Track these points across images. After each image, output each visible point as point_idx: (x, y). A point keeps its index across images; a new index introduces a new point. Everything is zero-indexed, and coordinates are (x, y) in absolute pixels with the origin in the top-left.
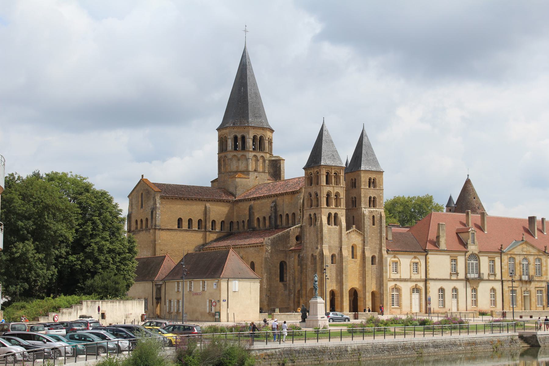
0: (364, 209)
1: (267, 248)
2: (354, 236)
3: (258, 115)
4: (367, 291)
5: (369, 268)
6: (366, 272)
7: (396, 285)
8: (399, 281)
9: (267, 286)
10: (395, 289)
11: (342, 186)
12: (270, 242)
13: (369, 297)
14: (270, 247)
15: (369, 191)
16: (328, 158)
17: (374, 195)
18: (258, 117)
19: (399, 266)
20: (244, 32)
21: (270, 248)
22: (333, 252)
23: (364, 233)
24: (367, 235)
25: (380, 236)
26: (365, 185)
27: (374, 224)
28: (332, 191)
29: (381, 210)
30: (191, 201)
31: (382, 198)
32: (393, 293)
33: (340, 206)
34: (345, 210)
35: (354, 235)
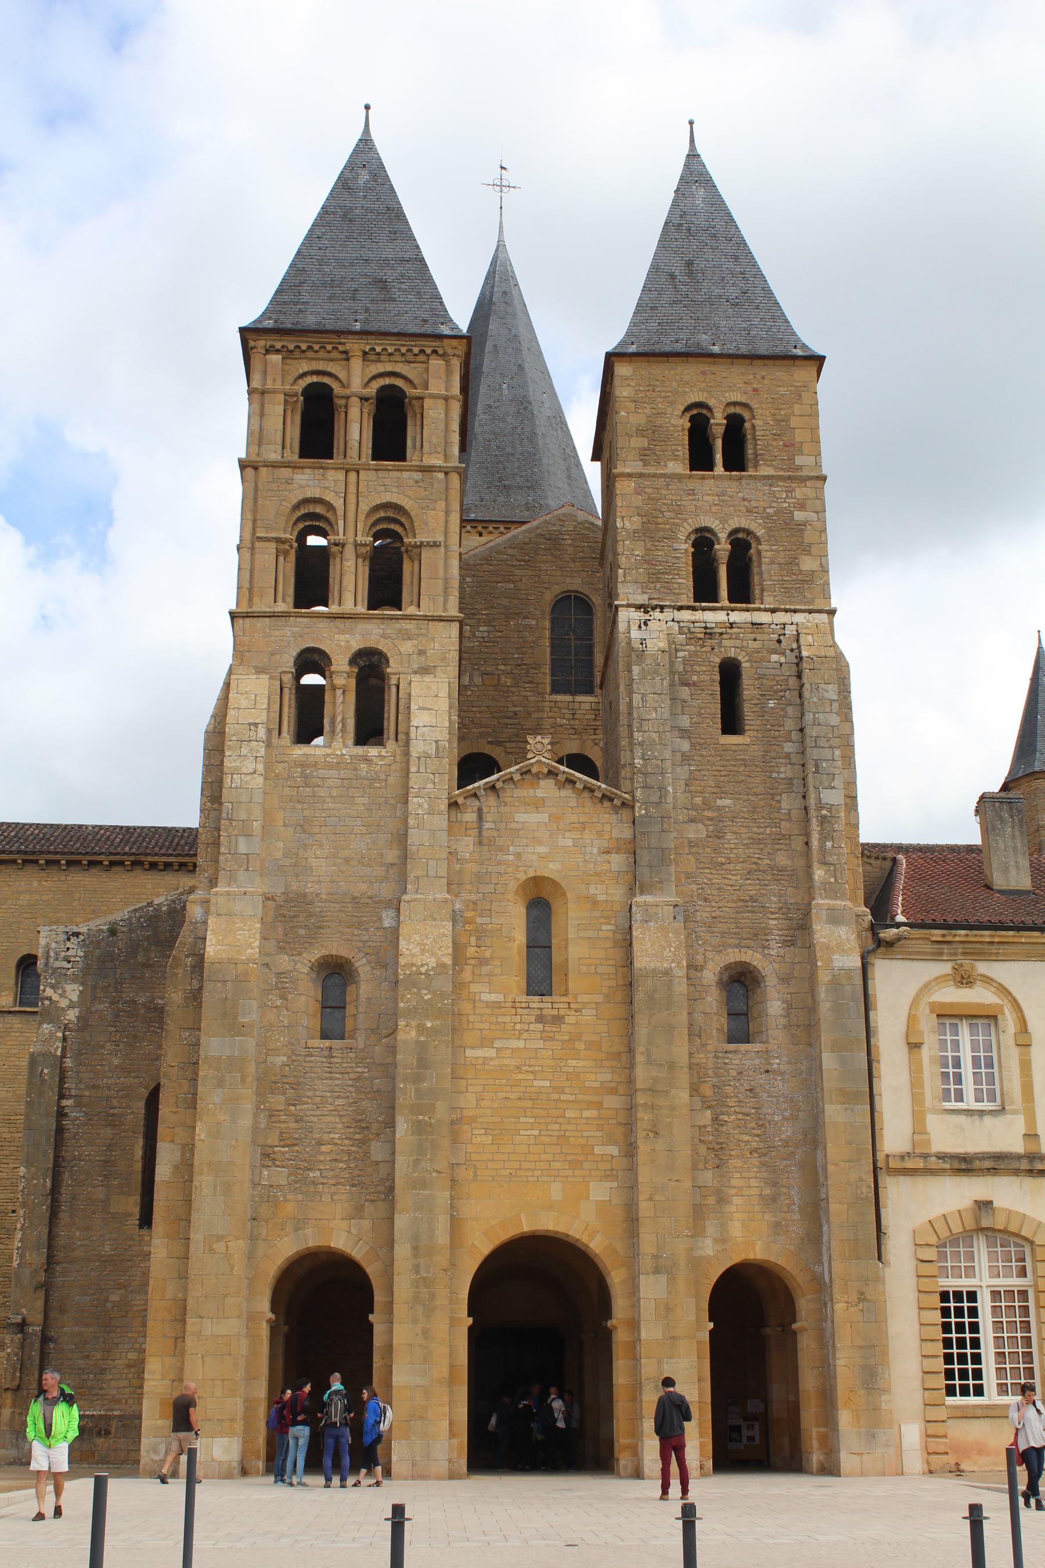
0: (637, 615)
1: (49, 992)
2: (544, 817)
3: (518, 479)
4: (646, 1263)
5: (672, 1066)
6: (641, 1099)
7: (984, 1206)
8: (1016, 1172)
9: (22, 1256)
10: (981, 1249)
11: (438, 461)
12: (76, 951)
13: (667, 1309)
14: (73, 991)
15: (692, 492)
16: (330, 298)
17: (735, 523)
18: (520, 488)
19: (1012, 1057)
20: (494, 194)
21: (75, 998)
22: (334, 946)
23: (632, 793)
24: (658, 804)
25: (796, 814)
26: (644, 455)
27: (731, 723)
28: (338, 503)
29: (799, 618)
30: (94, 871)
31: (809, 536)
32: (964, 1284)
33: (419, 606)
34: (455, 628)
35: (538, 805)
